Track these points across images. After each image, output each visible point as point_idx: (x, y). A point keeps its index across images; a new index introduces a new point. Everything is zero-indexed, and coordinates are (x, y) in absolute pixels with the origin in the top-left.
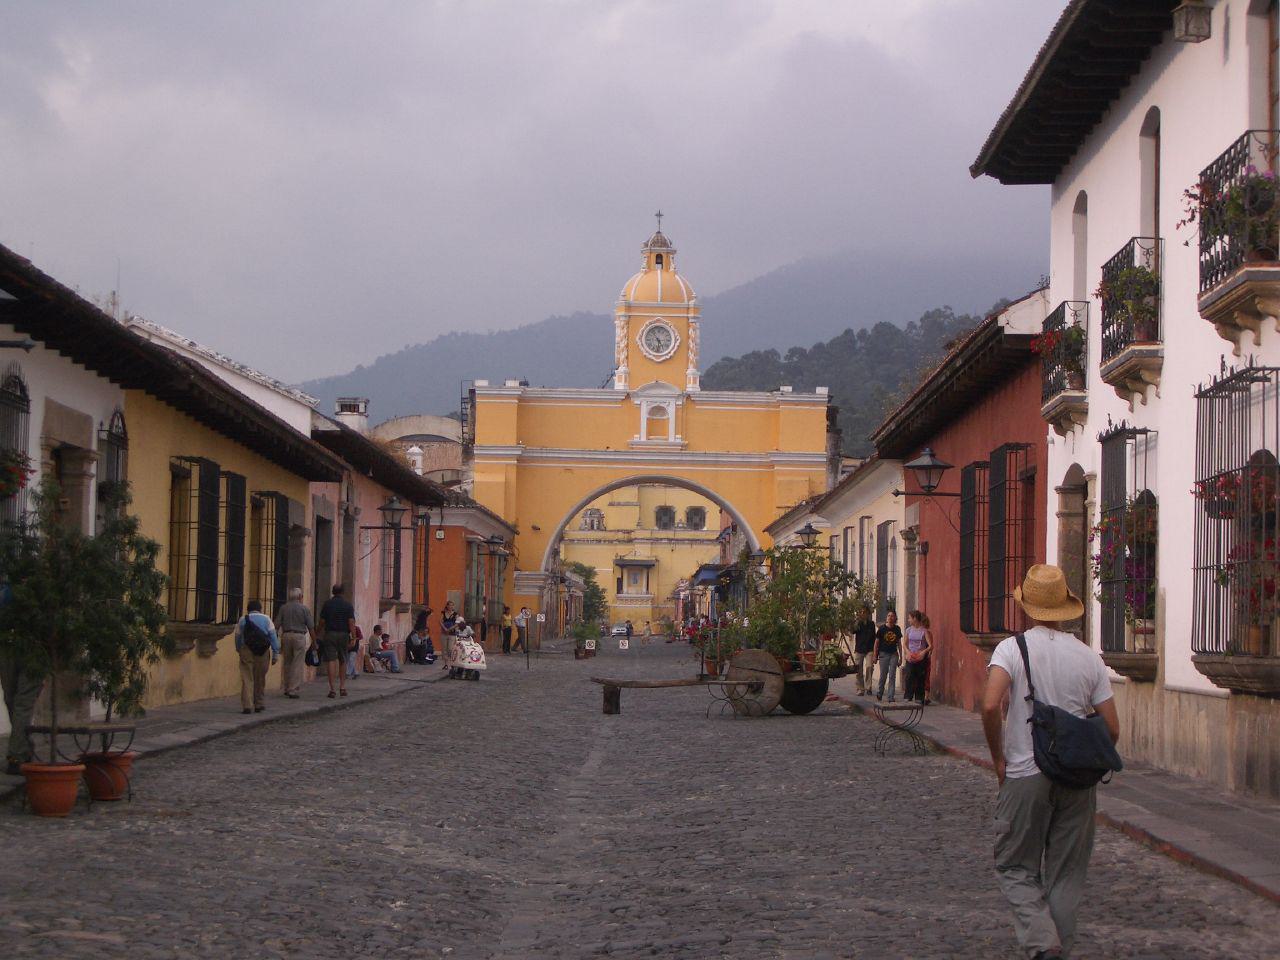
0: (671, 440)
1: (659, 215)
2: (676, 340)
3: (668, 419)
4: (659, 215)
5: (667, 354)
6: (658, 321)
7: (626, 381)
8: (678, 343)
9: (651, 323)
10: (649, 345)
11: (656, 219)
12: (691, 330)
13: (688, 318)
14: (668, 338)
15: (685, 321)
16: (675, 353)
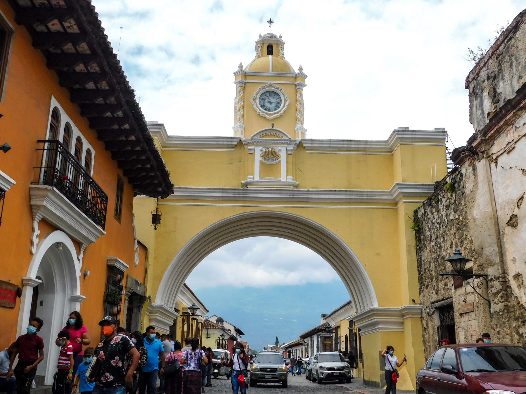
0: (283, 179)
1: (270, 22)
2: (286, 100)
3: (280, 162)
4: (270, 22)
5: (277, 113)
6: (270, 85)
7: (242, 134)
8: (287, 104)
9: (263, 88)
10: (263, 106)
11: (268, 24)
12: (298, 95)
13: (296, 85)
14: (278, 100)
15: (294, 86)
16: (284, 112)
